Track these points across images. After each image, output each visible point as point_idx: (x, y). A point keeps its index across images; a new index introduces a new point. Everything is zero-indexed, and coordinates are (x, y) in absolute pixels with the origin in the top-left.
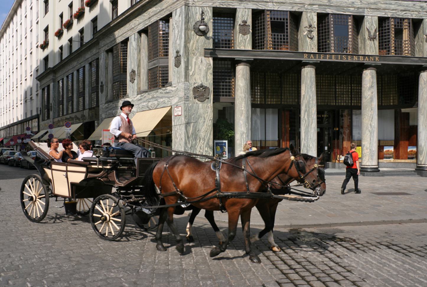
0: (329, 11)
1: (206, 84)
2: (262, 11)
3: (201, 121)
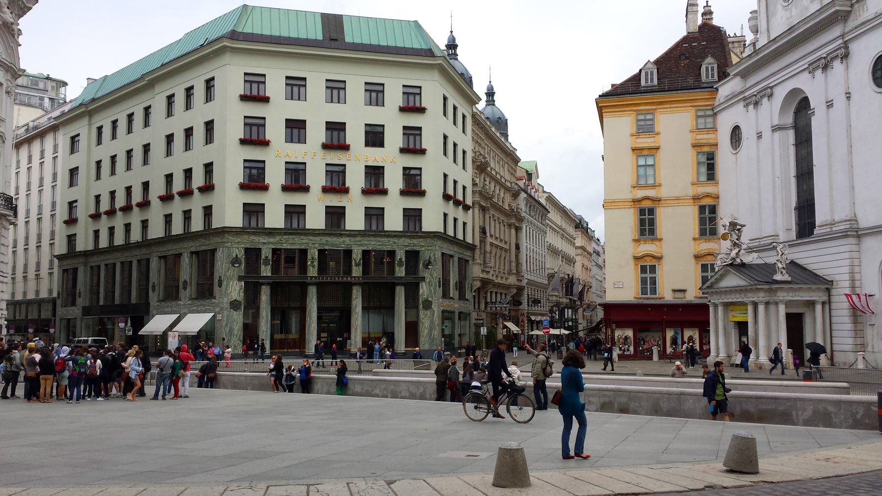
0: (327, 248)
1: (239, 299)
2: (280, 249)
3: (235, 323)
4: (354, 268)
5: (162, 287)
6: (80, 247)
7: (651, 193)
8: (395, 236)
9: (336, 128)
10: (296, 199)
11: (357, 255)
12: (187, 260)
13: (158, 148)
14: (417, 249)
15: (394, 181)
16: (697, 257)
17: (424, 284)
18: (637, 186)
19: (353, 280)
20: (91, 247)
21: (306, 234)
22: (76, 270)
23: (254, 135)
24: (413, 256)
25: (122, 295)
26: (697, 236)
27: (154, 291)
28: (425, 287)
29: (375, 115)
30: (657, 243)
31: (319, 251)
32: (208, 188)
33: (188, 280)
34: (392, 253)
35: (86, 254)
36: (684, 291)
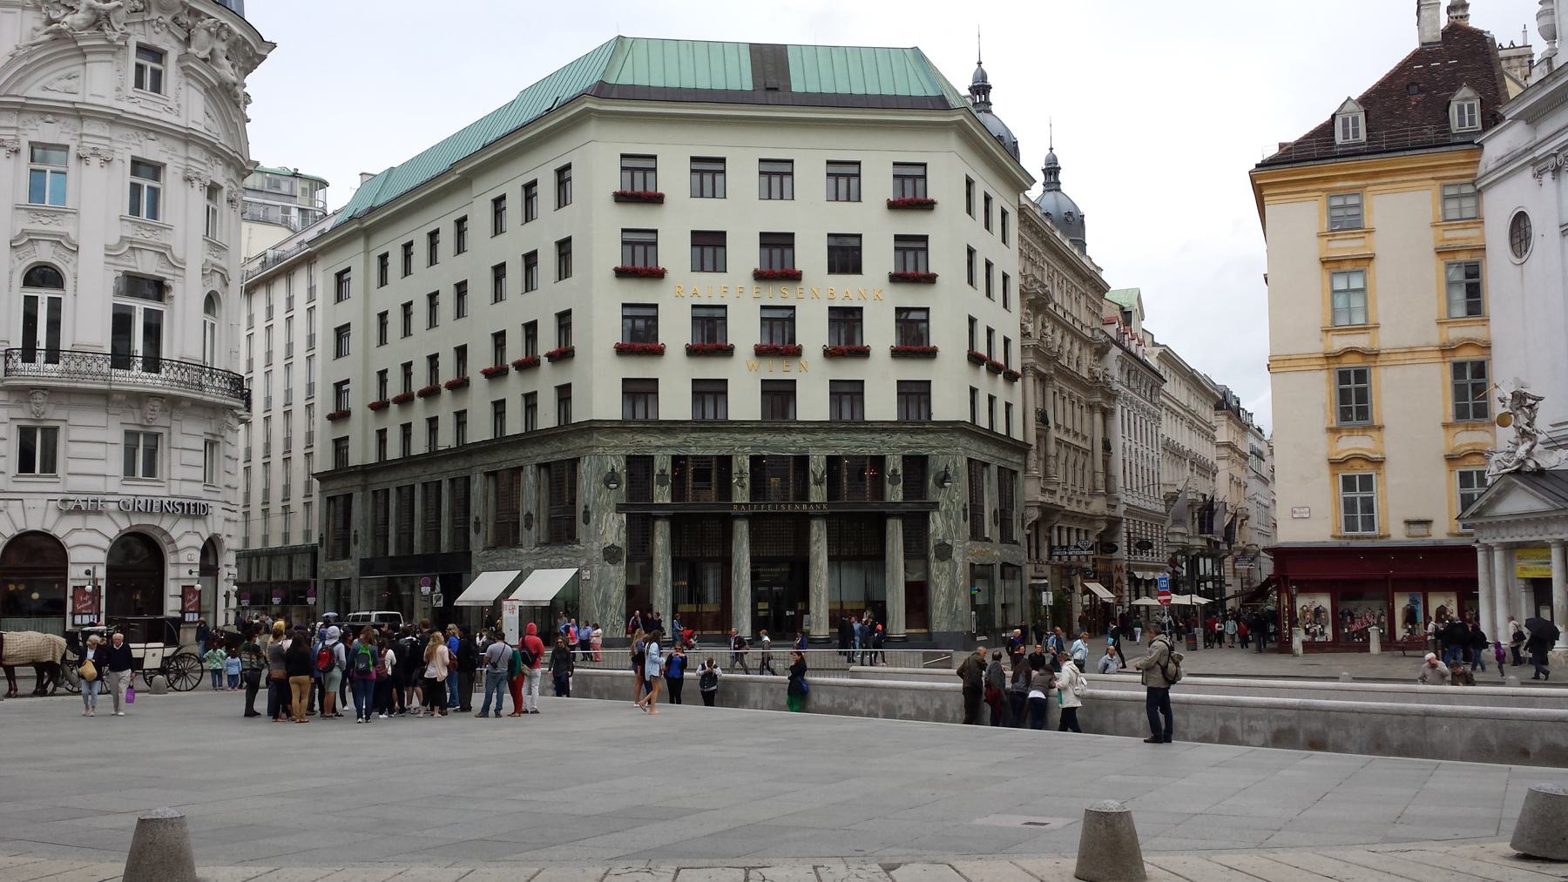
0: (765, 453)
2: (685, 458)
4: (813, 487)
5: (491, 524)
6: (355, 458)
7: (1360, 341)
8: (885, 430)
9: (777, 243)
10: (711, 369)
11: (817, 465)
12: (531, 478)
13: (480, 288)
14: (923, 452)
15: (879, 332)
16: (1451, 459)
17: (937, 514)
18: (1331, 329)
19: (812, 510)
20: (372, 458)
21: (728, 430)
22: (349, 497)
23: (639, 263)
24: (916, 465)
25: (425, 539)
26: (1451, 420)
27: (477, 531)
28: (938, 520)
29: (846, 218)
30: (1374, 434)
31: (752, 458)
32: (564, 355)
33: (533, 512)
34: (879, 461)
35: (365, 471)
36: (1427, 523)
